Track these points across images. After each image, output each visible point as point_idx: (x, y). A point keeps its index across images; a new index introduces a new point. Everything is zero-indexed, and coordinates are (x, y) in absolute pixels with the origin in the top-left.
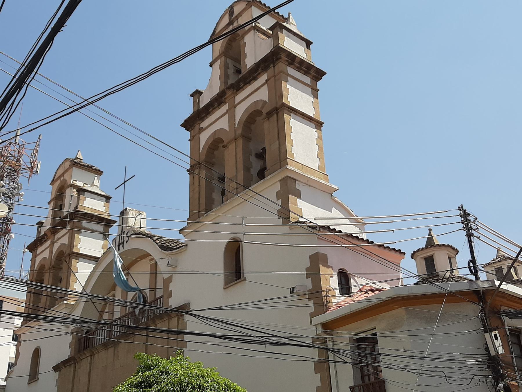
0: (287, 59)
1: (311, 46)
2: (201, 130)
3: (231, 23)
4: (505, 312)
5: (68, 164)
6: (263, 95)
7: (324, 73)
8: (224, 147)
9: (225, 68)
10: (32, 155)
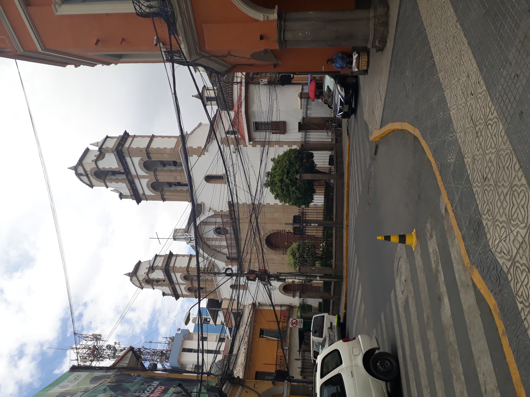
0: (120, 147)
1: (109, 136)
2: (144, 194)
3: (87, 175)
4: (253, 76)
5: (134, 278)
6: (137, 160)
7: (126, 131)
8: (157, 181)
9: (111, 181)
10: (87, 340)
